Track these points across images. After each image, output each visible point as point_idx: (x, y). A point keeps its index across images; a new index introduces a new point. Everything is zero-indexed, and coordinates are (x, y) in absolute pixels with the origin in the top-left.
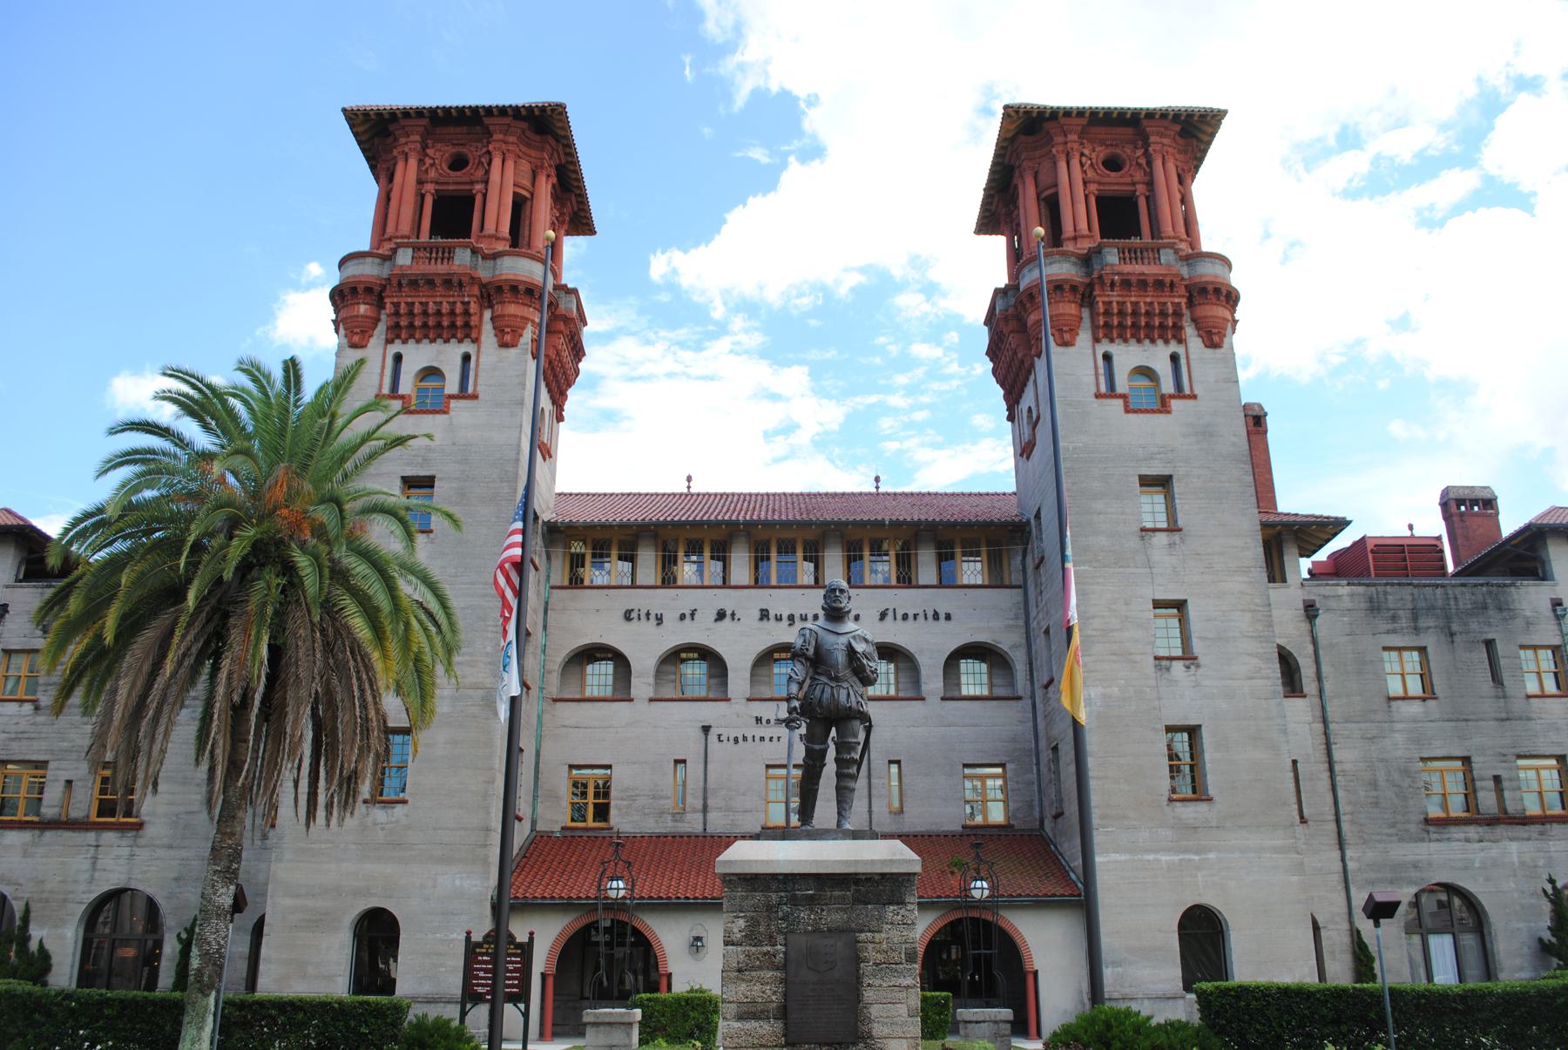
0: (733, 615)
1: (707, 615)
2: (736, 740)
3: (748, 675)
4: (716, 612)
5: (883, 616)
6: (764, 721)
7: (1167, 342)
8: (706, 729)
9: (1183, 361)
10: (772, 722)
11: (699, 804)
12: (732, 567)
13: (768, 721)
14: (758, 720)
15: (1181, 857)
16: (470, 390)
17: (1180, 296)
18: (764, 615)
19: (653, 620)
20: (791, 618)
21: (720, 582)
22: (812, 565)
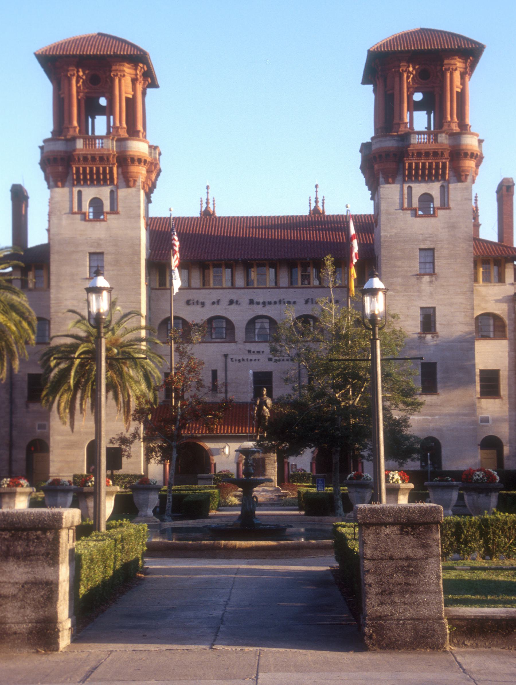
0: (237, 302)
1: (225, 302)
2: (239, 361)
3: (244, 330)
4: (228, 300)
5: (307, 302)
6: (252, 352)
7: (438, 181)
8: (226, 356)
9: (446, 190)
10: (256, 352)
11: (223, 390)
12: (236, 279)
13: (254, 352)
14: (249, 351)
15: (424, 417)
16: (115, 209)
17: (446, 159)
18: (251, 302)
19: (200, 306)
20: (264, 303)
21: (230, 284)
22: (273, 270)
